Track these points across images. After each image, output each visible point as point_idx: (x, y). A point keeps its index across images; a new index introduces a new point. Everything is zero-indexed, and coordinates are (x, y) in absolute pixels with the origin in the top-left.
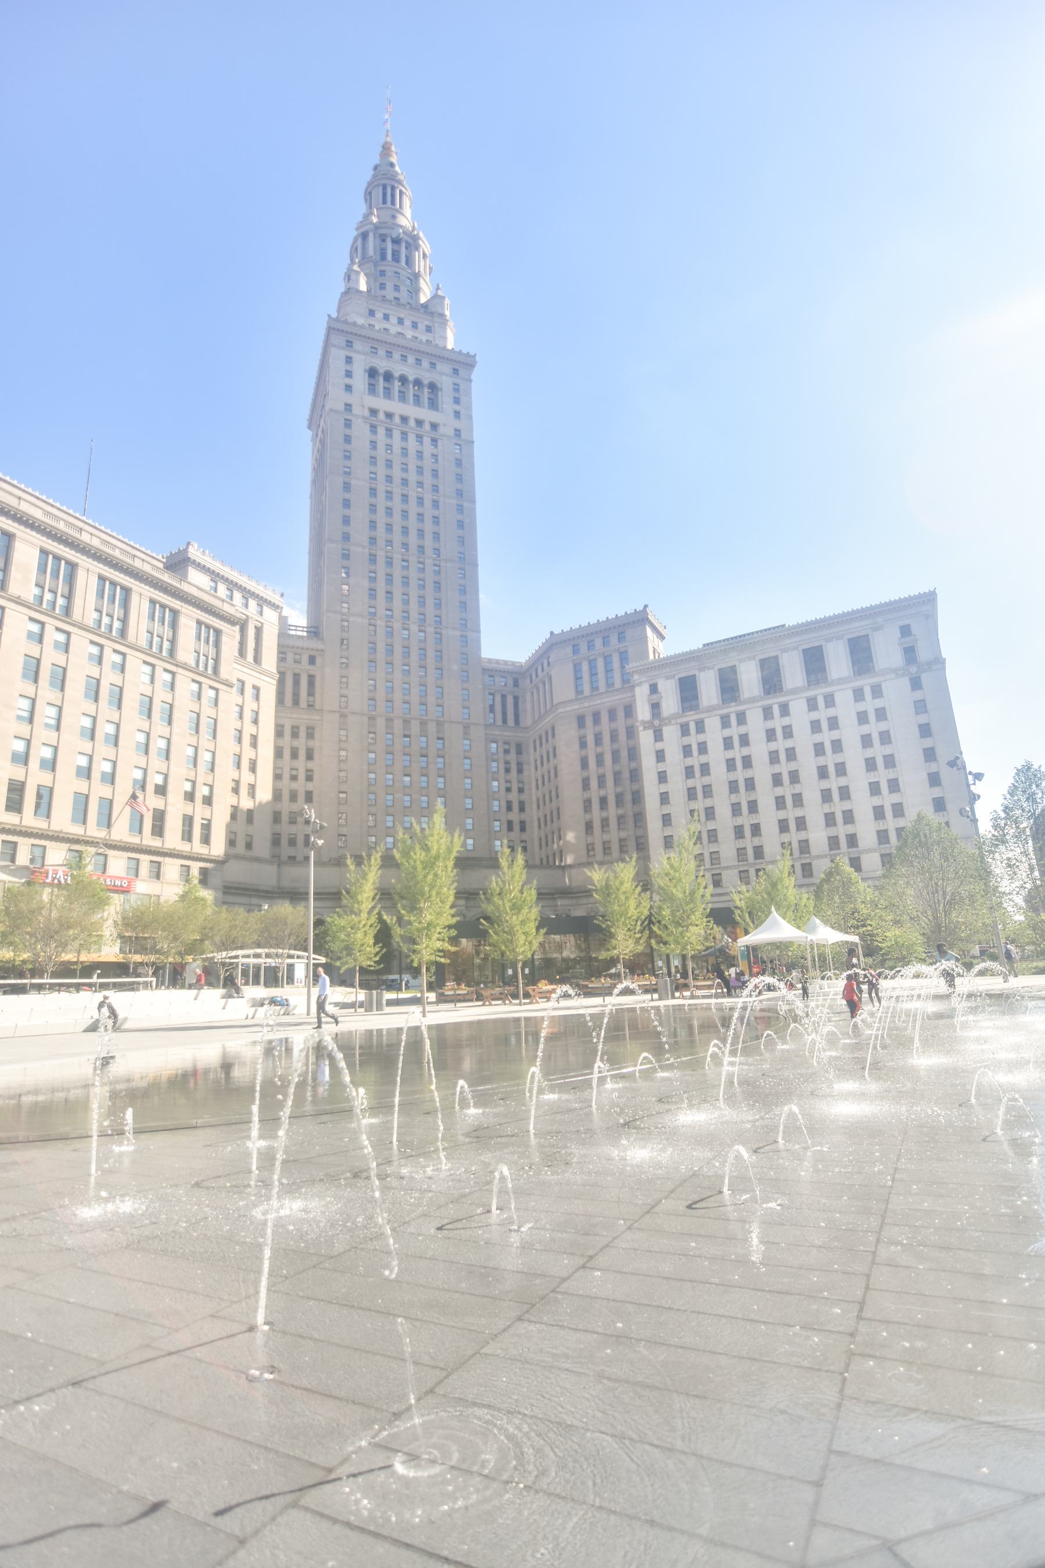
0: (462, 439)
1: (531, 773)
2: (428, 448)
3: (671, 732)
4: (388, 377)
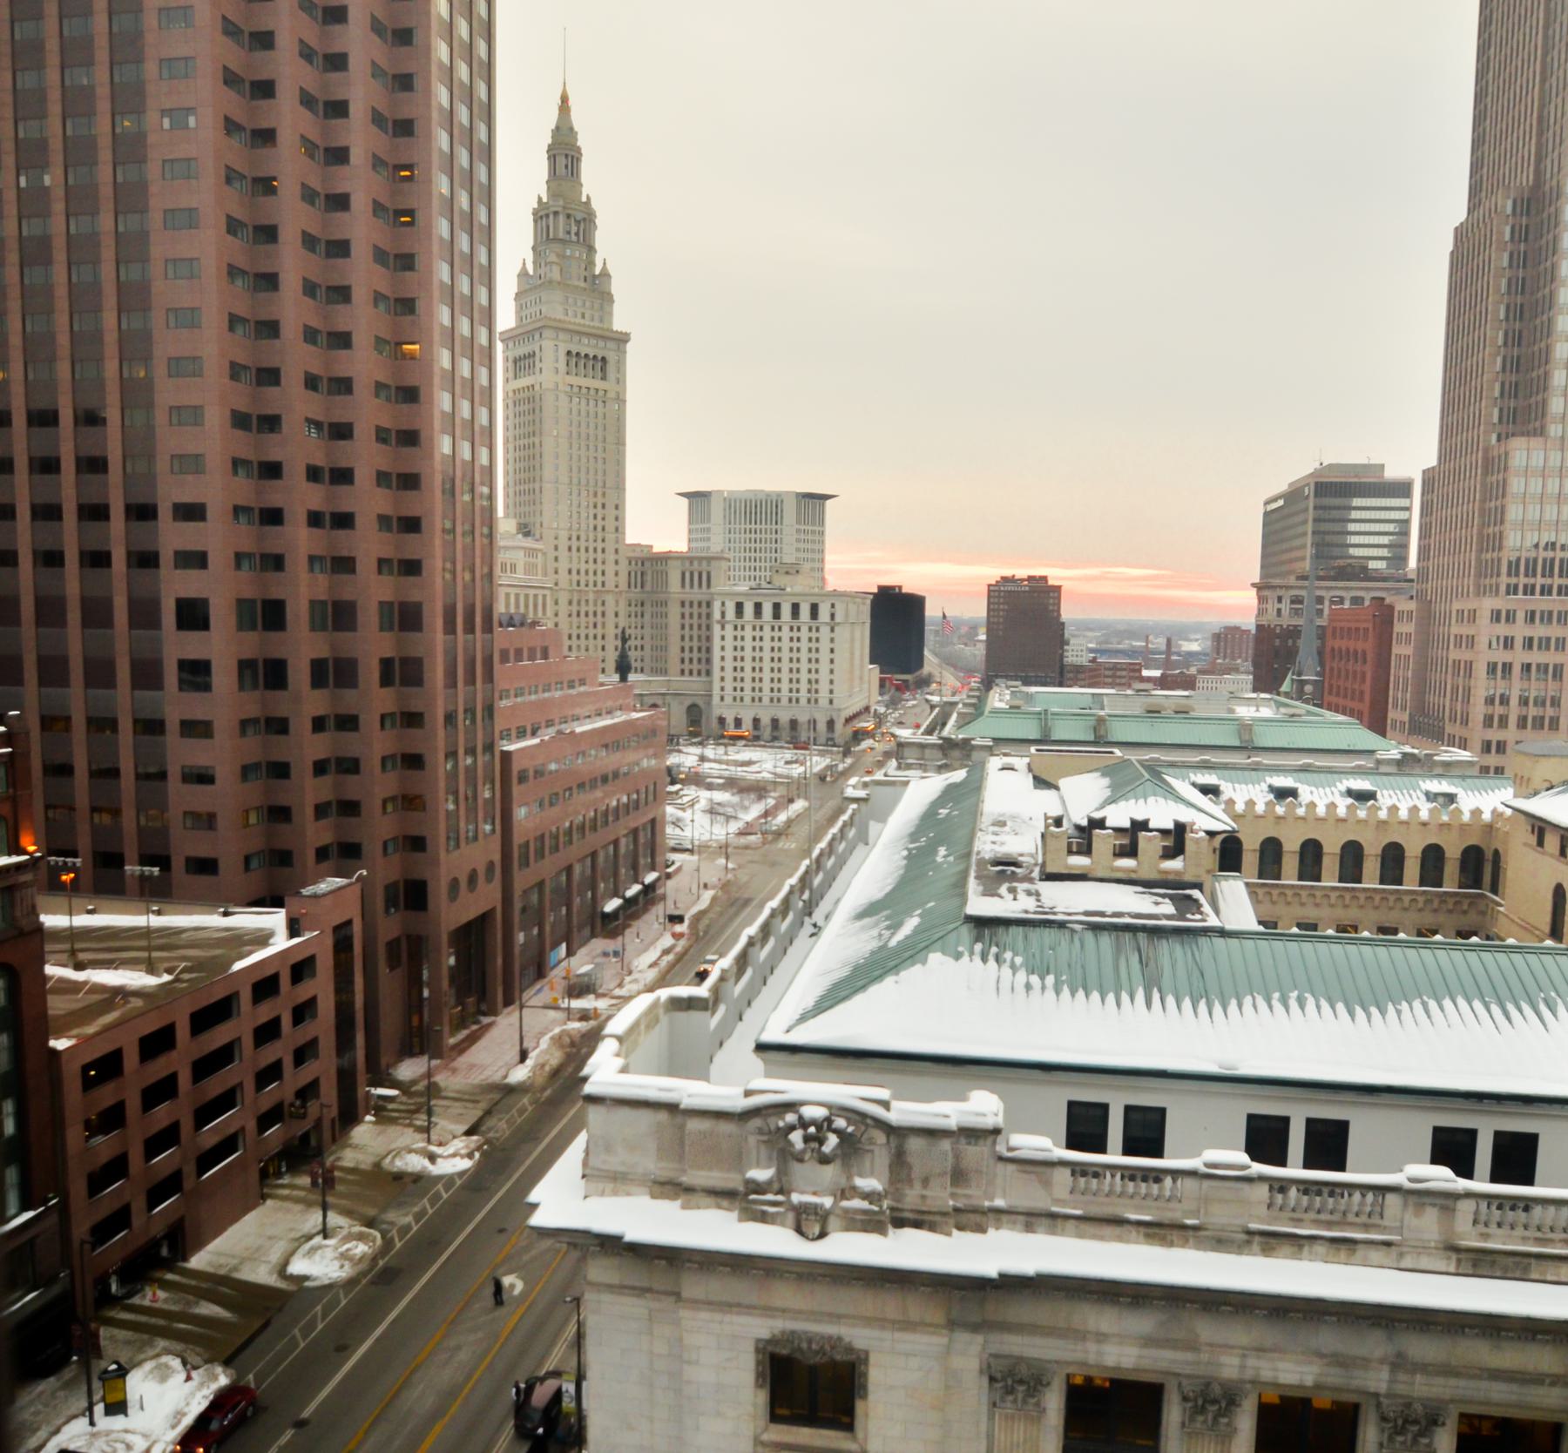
0: (621, 400)
1: (647, 616)
2: (600, 409)
3: (729, 628)
4: (578, 354)
